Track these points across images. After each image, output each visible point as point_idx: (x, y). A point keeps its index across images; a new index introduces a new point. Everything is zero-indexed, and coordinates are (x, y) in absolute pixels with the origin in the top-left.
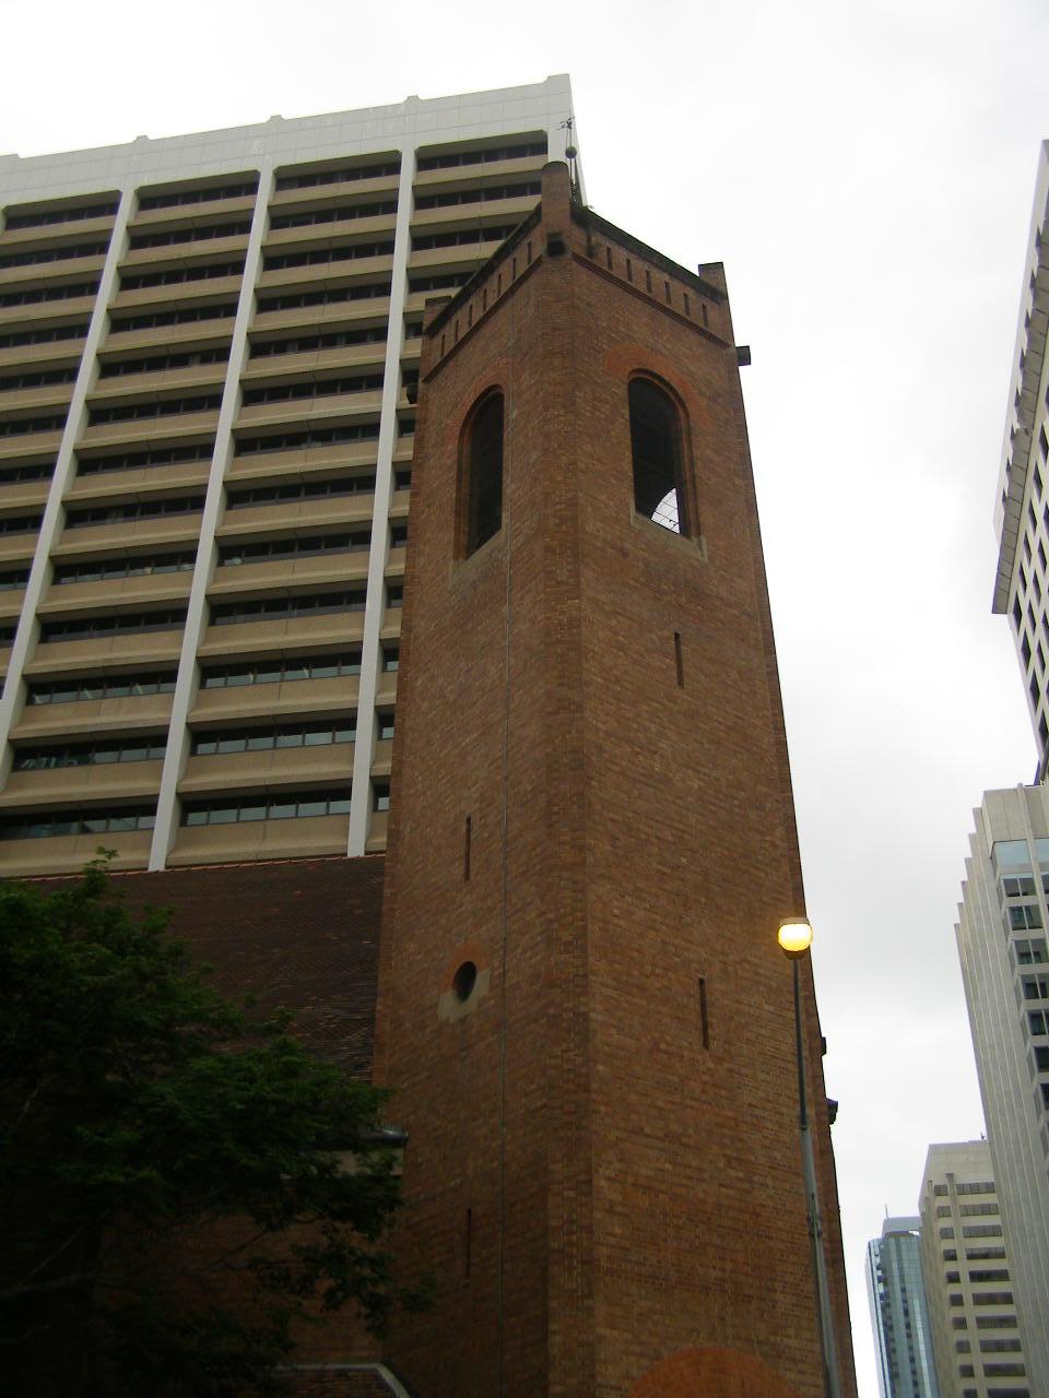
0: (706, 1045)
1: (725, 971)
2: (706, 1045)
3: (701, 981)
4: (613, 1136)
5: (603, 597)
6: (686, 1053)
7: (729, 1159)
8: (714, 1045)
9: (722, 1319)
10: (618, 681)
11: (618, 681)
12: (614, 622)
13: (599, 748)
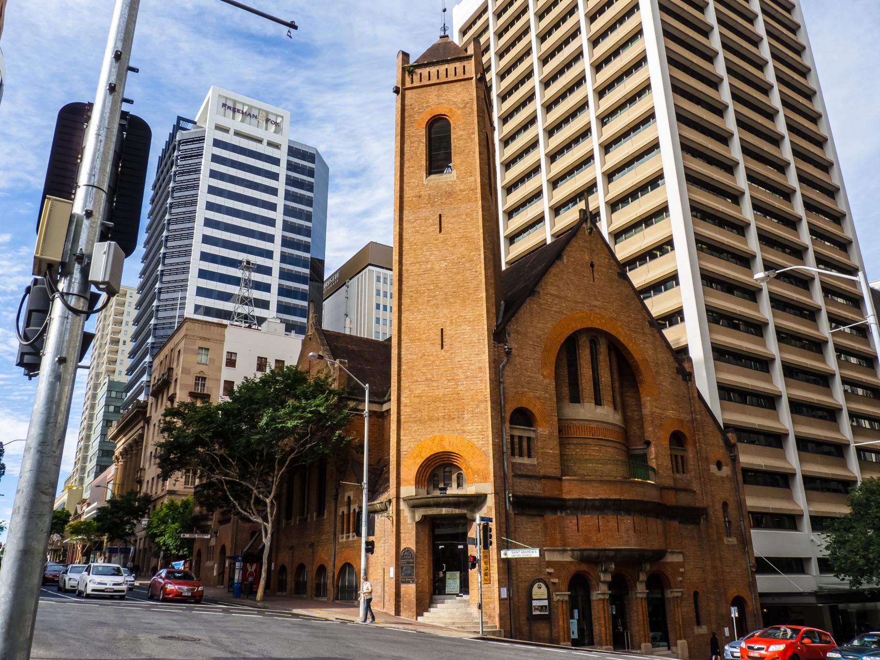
0: (442, 348)
1: (452, 323)
2: (442, 348)
7: (449, 380)
8: (445, 347)
10: (415, 244)
11: (415, 244)
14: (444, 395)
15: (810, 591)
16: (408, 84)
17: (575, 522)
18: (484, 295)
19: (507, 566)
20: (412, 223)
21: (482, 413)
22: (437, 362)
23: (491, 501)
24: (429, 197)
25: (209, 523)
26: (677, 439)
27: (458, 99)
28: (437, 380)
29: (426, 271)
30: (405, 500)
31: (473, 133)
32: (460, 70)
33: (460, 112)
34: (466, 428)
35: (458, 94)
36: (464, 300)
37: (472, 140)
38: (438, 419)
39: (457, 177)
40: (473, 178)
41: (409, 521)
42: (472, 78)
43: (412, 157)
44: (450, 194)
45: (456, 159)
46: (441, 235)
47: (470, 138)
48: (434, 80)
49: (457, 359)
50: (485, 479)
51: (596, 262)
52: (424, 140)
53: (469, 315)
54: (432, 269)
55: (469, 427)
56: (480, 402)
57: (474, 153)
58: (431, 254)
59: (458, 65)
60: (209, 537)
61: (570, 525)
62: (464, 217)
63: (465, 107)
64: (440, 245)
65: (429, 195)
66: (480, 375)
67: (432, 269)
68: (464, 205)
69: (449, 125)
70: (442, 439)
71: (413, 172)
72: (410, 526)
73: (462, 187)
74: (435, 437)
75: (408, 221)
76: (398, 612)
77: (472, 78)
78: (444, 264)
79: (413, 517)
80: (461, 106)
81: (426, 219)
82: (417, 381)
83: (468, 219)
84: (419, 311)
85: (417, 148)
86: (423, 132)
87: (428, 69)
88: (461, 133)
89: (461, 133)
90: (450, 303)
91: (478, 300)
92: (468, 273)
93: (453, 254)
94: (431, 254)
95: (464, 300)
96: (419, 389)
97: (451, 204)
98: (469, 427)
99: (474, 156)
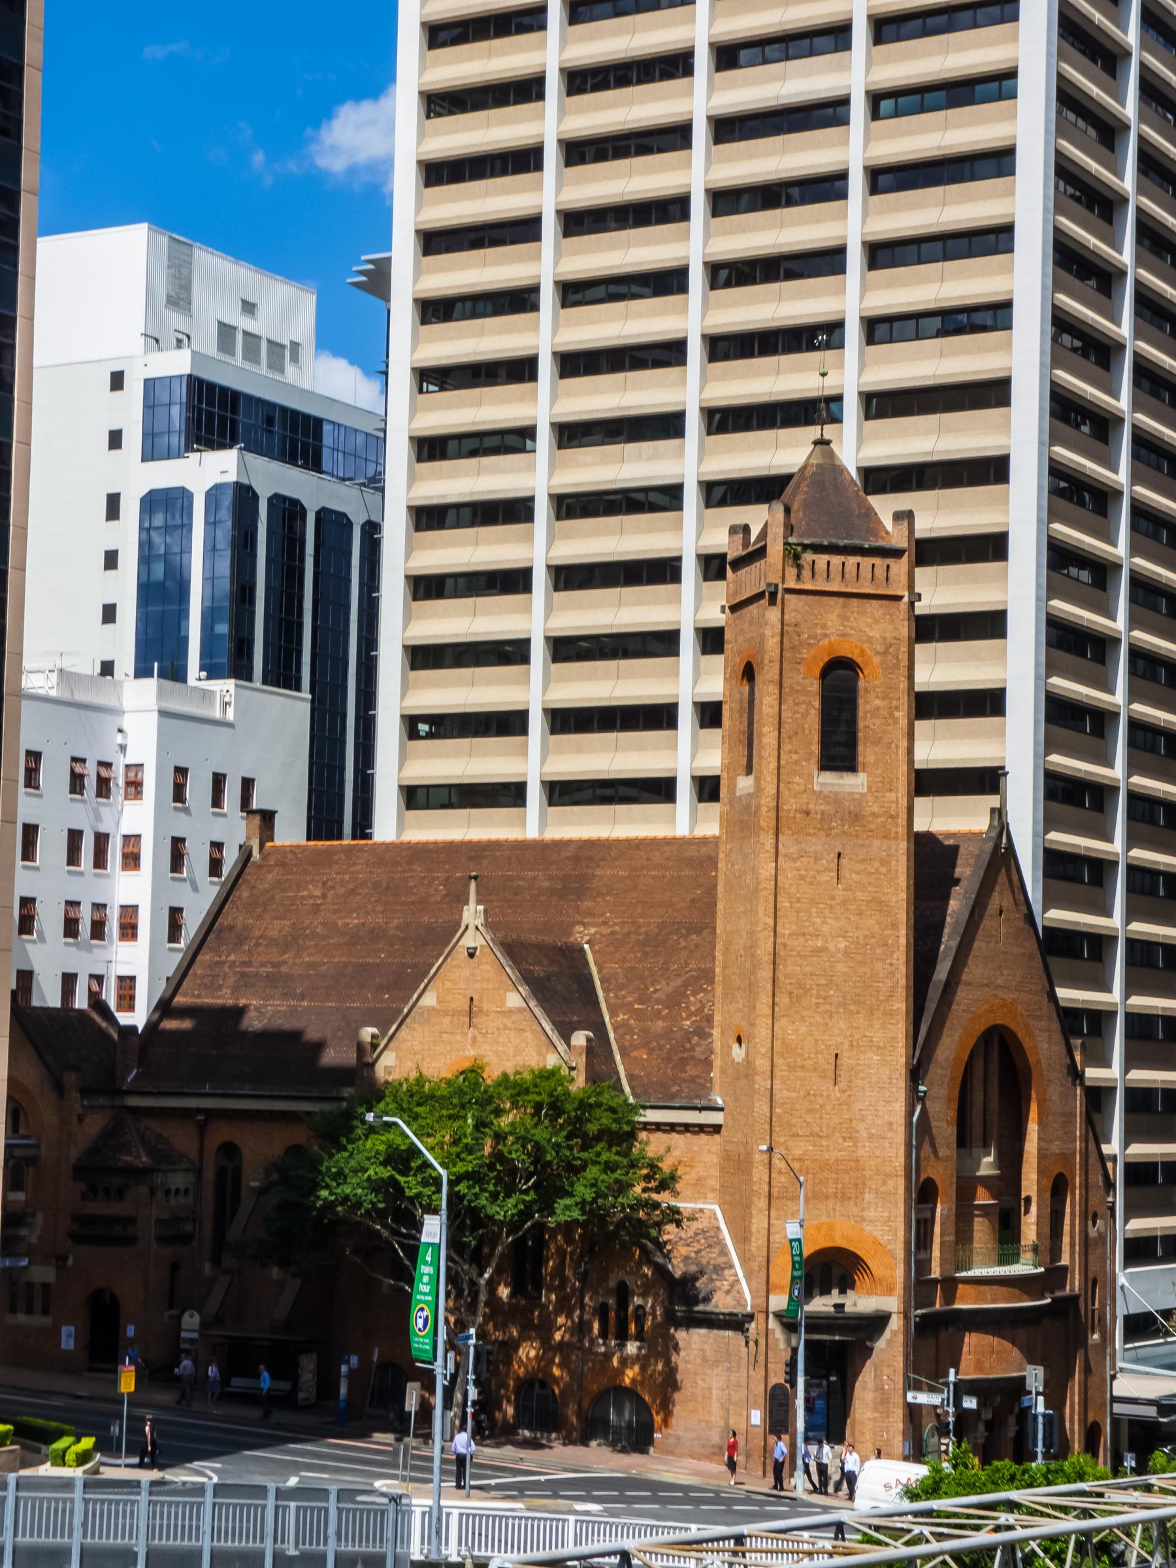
1: (852, 1045)
3: (837, 1055)
4: (782, 1140)
5: (792, 850)
6: (825, 1093)
7: (844, 1139)
8: (843, 1085)
9: (834, 1209)
12: (798, 863)
13: (785, 945)
14: (837, 1160)
15: (1152, 1396)
16: (792, 584)
18: (903, 1006)
19: (913, 1413)
20: (794, 860)
21: (889, 1193)
22: (828, 1108)
23: (895, 1323)
25: (23, 1232)
26: (1058, 1188)
27: (874, 633)
28: (827, 1137)
29: (817, 952)
30: (778, 1316)
31: (897, 708)
32: (880, 573)
33: (877, 660)
34: (867, 1214)
35: (877, 622)
37: (896, 721)
38: (827, 1198)
39: (869, 788)
40: (891, 796)
41: (782, 1345)
42: (902, 597)
43: (796, 733)
44: (856, 817)
45: (866, 753)
46: (840, 892)
47: (892, 715)
49: (858, 1106)
50: (889, 1291)
52: (817, 704)
53: (878, 1036)
54: (825, 949)
55: (871, 1214)
56: (888, 1176)
57: (897, 747)
58: (824, 923)
59: (877, 561)
60: (25, 1262)
62: (876, 864)
63: (886, 652)
64: (838, 909)
65: (823, 813)
66: (890, 1135)
67: (825, 949)
68: (877, 843)
70: (831, 1227)
71: (796, 763)
72: (784, 1354)
73: (875, 809)
74: (822, 1224)
75: (786, 855)
76: (764, 1475)
77: (902, 597)
78: (843, 944)
79: (788, 1341)
80: (880, 648)
81: (817, 859)
82: (798, 1135)
83: (884, 870)
84: (803, 1018)
85: (805, 715)
86: (815, 686)
87: (826, 557)
88: (877, 702)
89: (877, 702)
90: (851, 1012)
91: (891, 1014)
92: (879, 966)
93: (857, 928)
94: (824, 923)
95: (871, 1011)
96: (800, 1148)
97: (857, 836)
98: (871, 1214)
99: (897, 754)
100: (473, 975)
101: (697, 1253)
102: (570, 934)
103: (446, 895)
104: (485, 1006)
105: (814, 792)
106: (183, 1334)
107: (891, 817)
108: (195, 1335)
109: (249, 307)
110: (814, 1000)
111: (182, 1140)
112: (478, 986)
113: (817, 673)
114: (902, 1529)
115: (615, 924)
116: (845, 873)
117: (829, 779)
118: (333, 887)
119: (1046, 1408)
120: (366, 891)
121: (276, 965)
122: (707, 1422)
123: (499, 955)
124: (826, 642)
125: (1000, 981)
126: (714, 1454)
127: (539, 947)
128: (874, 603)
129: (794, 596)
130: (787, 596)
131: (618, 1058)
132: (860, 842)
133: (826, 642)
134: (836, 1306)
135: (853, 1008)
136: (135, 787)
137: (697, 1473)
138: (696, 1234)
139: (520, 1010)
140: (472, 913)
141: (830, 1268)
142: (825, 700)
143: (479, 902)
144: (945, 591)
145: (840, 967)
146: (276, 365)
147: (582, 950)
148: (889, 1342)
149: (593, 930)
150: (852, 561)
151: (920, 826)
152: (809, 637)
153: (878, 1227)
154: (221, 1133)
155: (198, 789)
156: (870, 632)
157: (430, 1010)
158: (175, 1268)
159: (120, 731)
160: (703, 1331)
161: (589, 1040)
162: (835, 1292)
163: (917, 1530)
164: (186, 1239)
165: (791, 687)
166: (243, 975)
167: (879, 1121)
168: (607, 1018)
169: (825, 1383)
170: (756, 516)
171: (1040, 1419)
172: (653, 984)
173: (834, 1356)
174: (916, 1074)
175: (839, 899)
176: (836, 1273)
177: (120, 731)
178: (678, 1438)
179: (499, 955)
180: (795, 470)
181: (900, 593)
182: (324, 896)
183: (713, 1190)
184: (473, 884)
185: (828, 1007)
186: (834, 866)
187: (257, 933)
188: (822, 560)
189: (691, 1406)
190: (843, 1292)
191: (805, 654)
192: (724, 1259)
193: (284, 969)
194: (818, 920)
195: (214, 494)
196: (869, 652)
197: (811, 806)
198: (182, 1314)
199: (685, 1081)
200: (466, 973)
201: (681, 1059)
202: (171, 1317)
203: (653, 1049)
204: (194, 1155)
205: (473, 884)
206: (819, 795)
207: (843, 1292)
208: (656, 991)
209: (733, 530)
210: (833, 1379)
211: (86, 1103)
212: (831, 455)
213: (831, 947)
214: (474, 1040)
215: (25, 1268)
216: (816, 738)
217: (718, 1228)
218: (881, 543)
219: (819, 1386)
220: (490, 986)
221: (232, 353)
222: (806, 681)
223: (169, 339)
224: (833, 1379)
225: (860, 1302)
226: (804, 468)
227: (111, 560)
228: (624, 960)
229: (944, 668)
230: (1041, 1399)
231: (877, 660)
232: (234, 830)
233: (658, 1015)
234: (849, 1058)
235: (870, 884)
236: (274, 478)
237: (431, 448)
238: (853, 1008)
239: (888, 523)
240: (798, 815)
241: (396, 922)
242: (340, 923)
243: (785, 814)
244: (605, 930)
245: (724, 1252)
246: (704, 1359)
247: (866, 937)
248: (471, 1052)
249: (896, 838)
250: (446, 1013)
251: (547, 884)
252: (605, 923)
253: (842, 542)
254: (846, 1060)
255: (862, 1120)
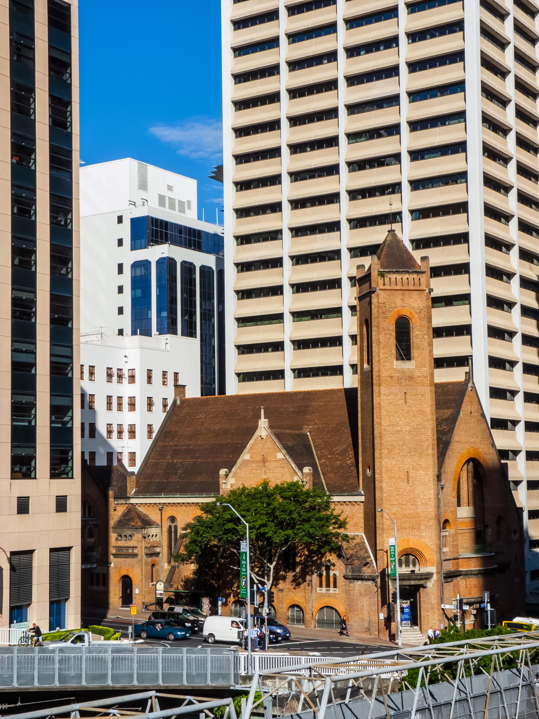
1: (413, 468)
4: (387, 507)
5: (387, 392)
7: (412, 505)
8: (410, 484)
13: (385, 430)
14: (409, 514)
16: (382, 287)
17: (465, 583)
20: (387, 396)
22: (405, 493)
24: (398, 379)
25: (94, 554)
26: (499, 520)
29: (398, 432)
31: (425, 335)
32: (417, 281)
33: (416, 316)
35: (416, 301)
36: (420, 454)
38: (406, 529)
39: (416, 366)
40: (425, 369)
44: (411, 378)
45: (415, 353)
47: (423, 337)
48: (399, 287)
49: (417, 492)
50: (432, 565)
51: (473, 410)
54: (401, 431)
58: (400, 420)
59: (415, 276)
60: (95, 566)
61: (462, 585)
62: (420, 396)
63: (420, 313)
65: (398, 377)
66: (430, 503)
67: (401, 431)
69: (408, 323)
70: (408, 541)
71: (386, 358)
73: (419, 374)
81: (396, 395)
83: (423, 398)
85: (389, 339)
86: (393, 327)
88: (418, 332)
89: (418, 332)
90: (412, 455)
93: (414, 422)
94: (400, 420)
95: (420, 454)
96: (395, 509)
97: (412, 386)
100: (264, 446)
101: (357, 552)
102: (301, 429)
103: (253, 416)
104: (269, 459)
105: (394, 369)
106: (157, 592)
107: (425, 377)
108: (162, 592)
109: (170, 188)
110: (398, 451)
111: (153, 515)
112: (266, 451)
113: (394, 322)
114: (420, 656)
115: (319, 424)
116: (408, 400)
117: (400, 363)
118: (209, 414)
119: (491, 607)
120: (222, 415)
121: (188, 446)
122: (363, 619)
123: (273, 438)
124: (396, 309)
125: (472, 440)
126: (366, 631)
127: (289, 434)
128: (415, 293)
129: (383, 291)
130: (380, 292)
131: (322, 477)
132: (413, 388)
133: (396, 309)
134: (411, 571)
135: (413, 453)
136: (132, 378)
137: (360, 639)
138: (355, 545)
139: (283, 459)
140: (263, 422)
141: (410, 556)
142: (397, 332)
143: (265, 418)
144: (443, 286)
145: (407, 437)
146: (182, 210)
147: (307, 435)
148: (433, 585)
149: (311, 427)
150: (405, 276)
151: (437, 380)
152: (389, 308)
153: (426, 540)
154: (168, 512)
155: (157, 377)
156: (413, 305)
157: (247, 461)
158: (153, 565)
159: (125, 356)
160: (360, 582)
161: (310, 470)
162: (411, 566)
163: (426, 656)
164: (157, 554)
165: (383, 328)
166: (175, 450)
167: (426, 498)
168: (317, 462)
169: (409, 601)
170: (367, 261)
171: (489, 612)
172: (335, 447)
173: (411, 592)
174: (439, 478)
175: (406, 411)
176: (411, 558)
177: (125, 356)
178: (352, 626)
179: (273, 438)
180: (381, 242)
181: (424, 288)
182: (205, 418)
183: (361, 527)
184: (262, 411)
185: (403, 453)
186: (403, 398)
187: (180, 434)
188: (393, 277)
189: (356, 613)
190: (414, 565)
191: (388, 315)
192: (367, 554)
193: (191, 447)
194: (398, 419)
195: (160, 262)
196: (413, 313)
197: (393, 374)
198: (157, 584)
199: (349, 485)
200: (261, 446)
201: (348, 476)
202: (153, 585)
203: (336, 473)
204: (159, 522)
205: (262, 411)
206: (396, 370)
207: (414, 565)
208: (336, 450)
209: (359, 267)
210: (412, 600)
211: (116, 502)
212: (395, 236)
213: (404, 429)
214: (265, 472)
215: (95, 568)
216: (394, 347)
217: (364, 542)
218: (416, 270)
219: (406, 603)
220: (271, 451)
221: (164, 206)
222: (389, 325)
223: (139, 203)
224: (412, 600)
225: (420, 569)
226: (385, 241)
227: (120, 290)
228: (323, 438)
229: (443, 317)
230: (489, 605)
231: (416, 316)
232: (170, 394)
233: (337, 459)
234: (413, 473)
235: (418, 404)
236: (181, 254)
237: (244, 240)
238: (413, 453)
239: (419, 262)
240: (388, 378)
241: (234, 427)
242: (212, 428)
243: (383, 378)
244: (316, 427)
245: (367, 552)
246: (361, 594)
247: (417, 425)
248: (264, 477)
249: (427, 385)
250: (254, 462)
251: (292, 410)
252: (315, 424)
253: (400, 270)
254: (412, 474)
255: (419, 498)
